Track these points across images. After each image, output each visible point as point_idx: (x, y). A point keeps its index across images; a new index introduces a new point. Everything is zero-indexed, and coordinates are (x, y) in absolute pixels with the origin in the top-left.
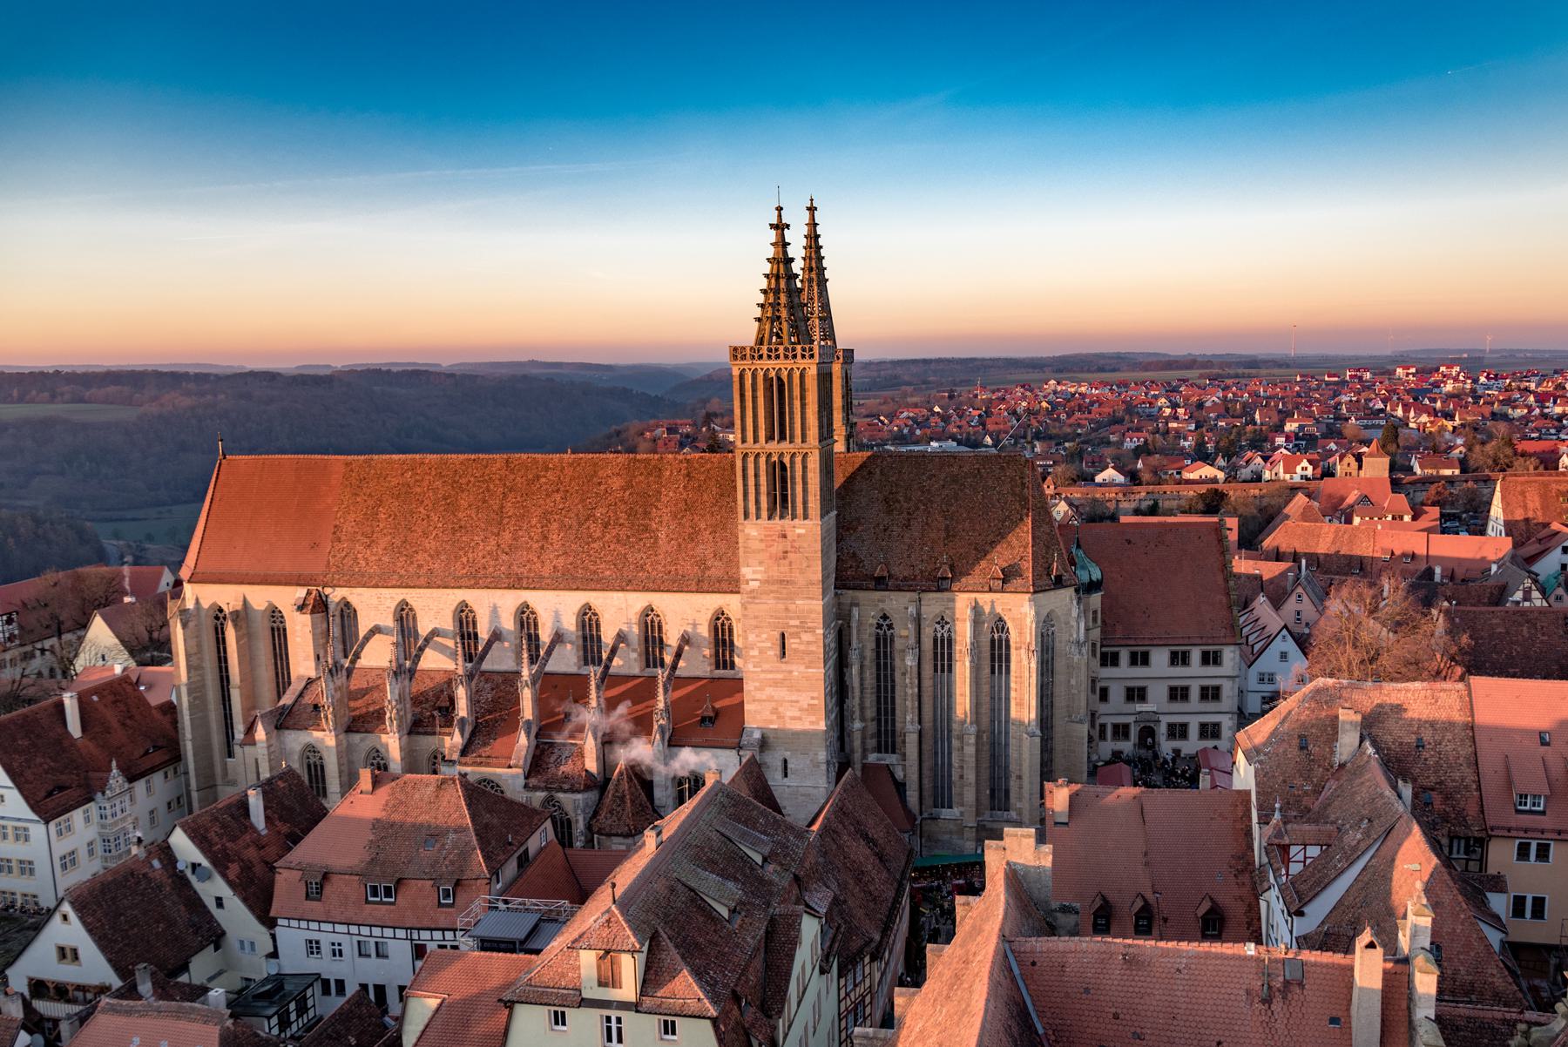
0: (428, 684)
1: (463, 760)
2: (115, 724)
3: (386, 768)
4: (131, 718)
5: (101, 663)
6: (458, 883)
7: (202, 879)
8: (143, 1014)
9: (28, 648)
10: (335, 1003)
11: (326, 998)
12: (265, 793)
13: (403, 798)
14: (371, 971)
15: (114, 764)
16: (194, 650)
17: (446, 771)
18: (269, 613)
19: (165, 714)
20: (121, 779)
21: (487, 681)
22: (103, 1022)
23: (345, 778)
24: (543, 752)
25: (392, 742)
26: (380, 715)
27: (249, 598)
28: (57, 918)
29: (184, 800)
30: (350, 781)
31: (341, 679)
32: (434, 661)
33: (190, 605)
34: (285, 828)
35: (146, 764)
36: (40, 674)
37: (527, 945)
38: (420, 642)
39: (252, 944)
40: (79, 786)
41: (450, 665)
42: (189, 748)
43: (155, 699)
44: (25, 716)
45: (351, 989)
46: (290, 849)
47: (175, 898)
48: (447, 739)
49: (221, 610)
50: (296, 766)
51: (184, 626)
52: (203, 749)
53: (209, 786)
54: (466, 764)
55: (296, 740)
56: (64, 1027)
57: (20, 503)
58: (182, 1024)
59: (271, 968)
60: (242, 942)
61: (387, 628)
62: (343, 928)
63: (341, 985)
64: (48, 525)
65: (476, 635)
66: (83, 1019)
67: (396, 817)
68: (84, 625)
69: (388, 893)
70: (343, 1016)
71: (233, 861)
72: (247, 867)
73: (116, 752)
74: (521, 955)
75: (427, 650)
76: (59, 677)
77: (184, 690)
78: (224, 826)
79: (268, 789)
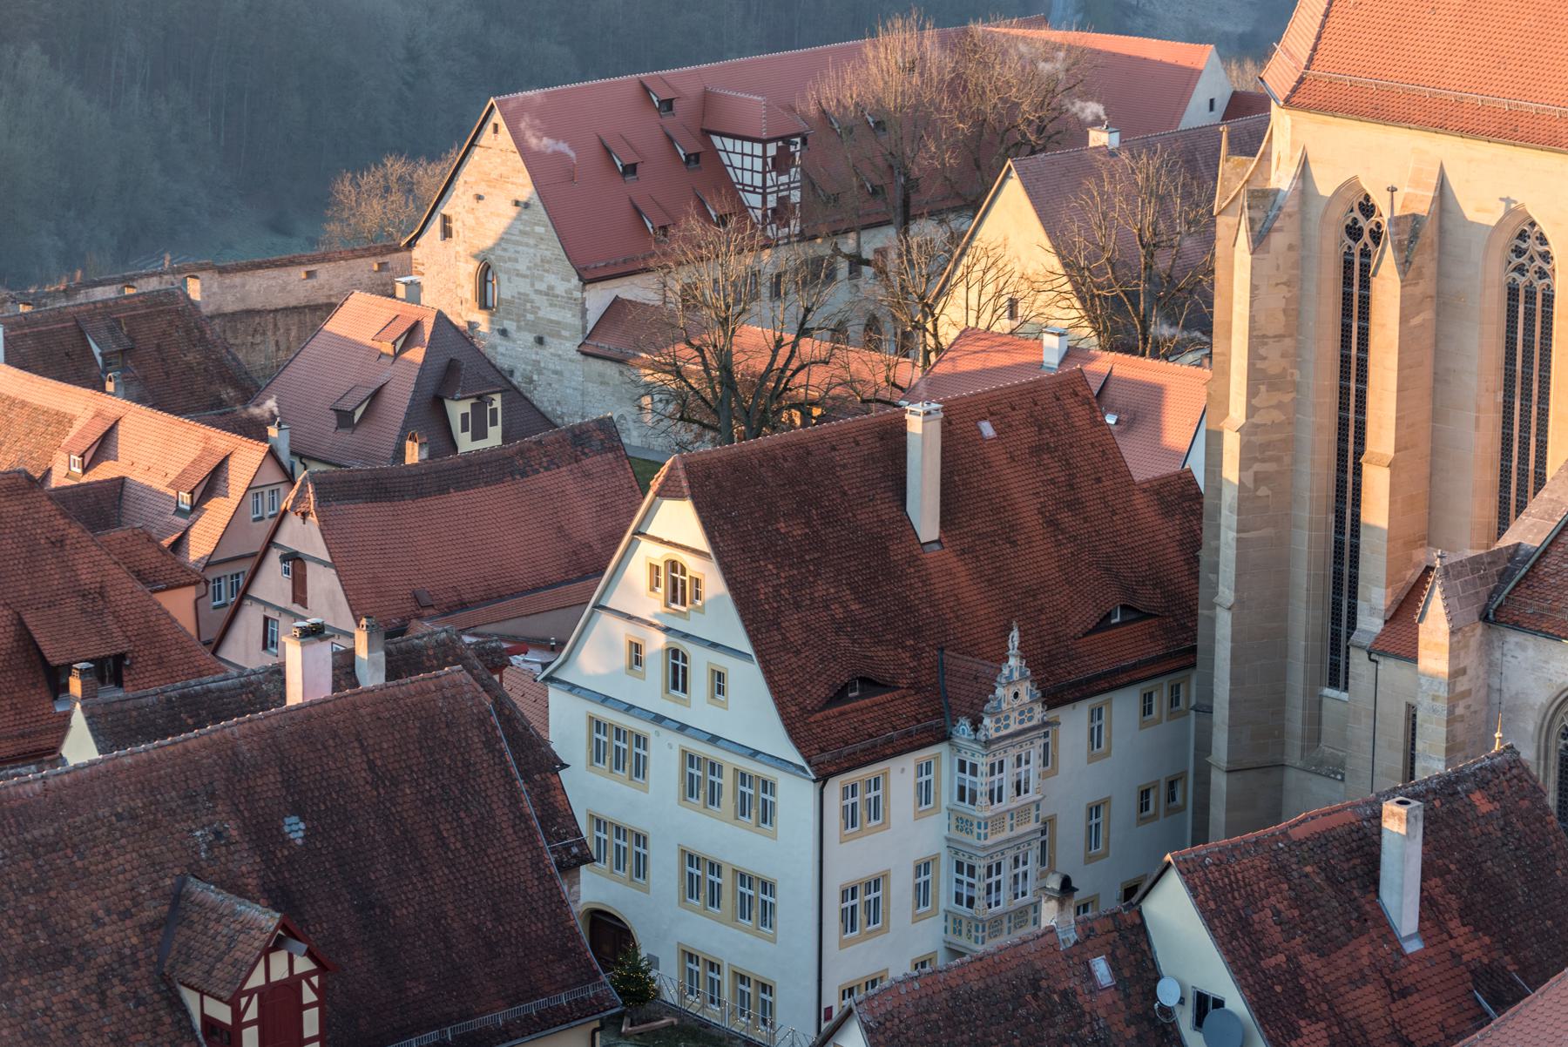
4: (1074, 505)
5: (1004, 325)
9: (821, 248)
15: (1015, 637)
16: (1277, 325)
18: (1506, 238)
19: (1167, 509)
20: (1025, 689)
33: (1282, 178)
34: (1474, 949)
40: (916, 687)
43: (1143, 466)
49: (1367, 209)
51: (1259, 240)
52: (1262, 649)
68: (970, 200)
71: (1314, 1017)
78: (1299, 900)
79: (1443, 808)
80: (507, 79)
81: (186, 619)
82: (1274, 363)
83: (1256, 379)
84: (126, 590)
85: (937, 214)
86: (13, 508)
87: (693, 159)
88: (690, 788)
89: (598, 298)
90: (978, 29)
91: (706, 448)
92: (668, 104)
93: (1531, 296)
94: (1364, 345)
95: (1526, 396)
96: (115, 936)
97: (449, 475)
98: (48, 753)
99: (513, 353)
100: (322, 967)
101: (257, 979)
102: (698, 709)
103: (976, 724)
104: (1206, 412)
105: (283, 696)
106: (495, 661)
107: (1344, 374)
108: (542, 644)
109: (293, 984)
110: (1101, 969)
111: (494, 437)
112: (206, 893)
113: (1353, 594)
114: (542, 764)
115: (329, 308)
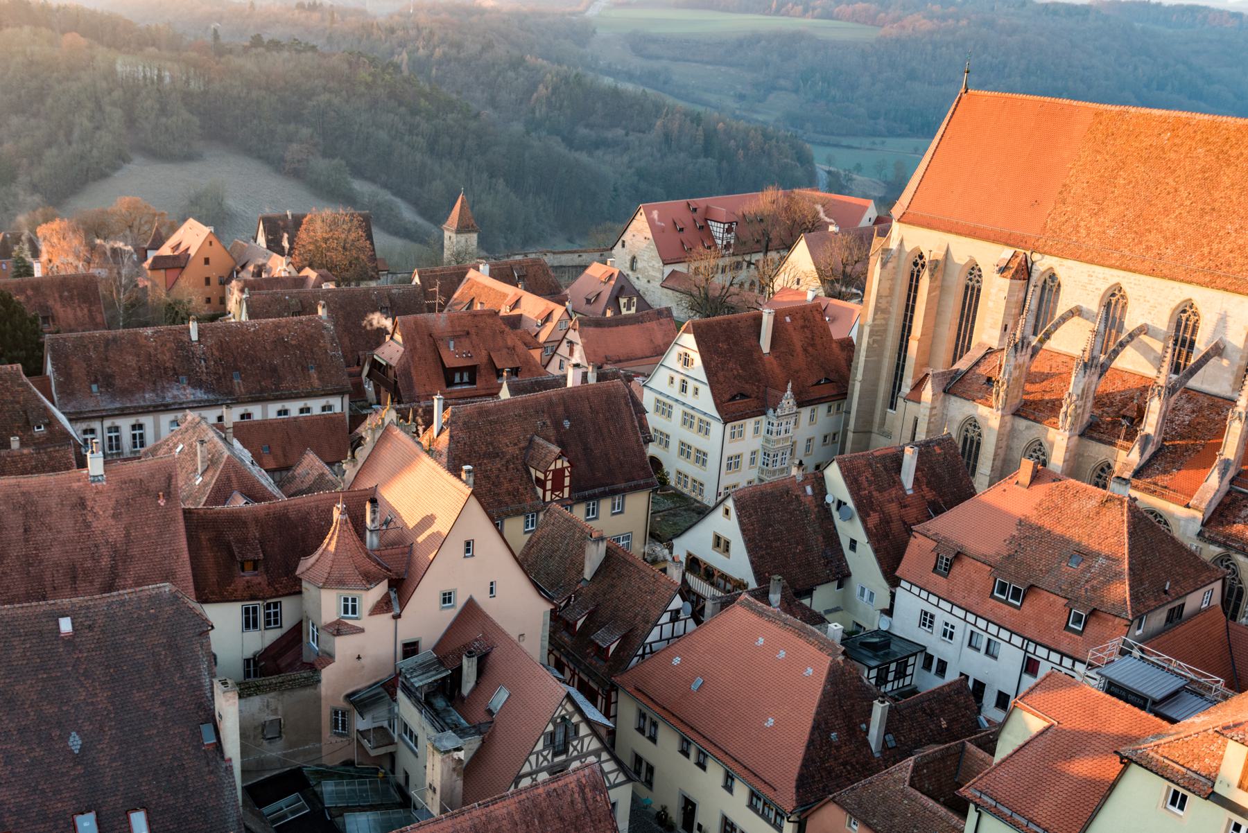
0: (1119, 386)
1: (1134, 482)
2: (799, 348)
3: (1044, 464)
4: (813, 345)
5: (795, 287)
6: (1093, 612)
7: (843, 518)
8: (772, 619)
9: (740, 259)
10: (930, 682)
11: (925, 672)
12: (920, 455)
13: (1060, 502)
14: (975, 665)
16: (885, 292)
17: (1115, 488)
18: (968, 269)
20: (792, 401)
21: (1189, 400)
22: (740, 615)
23: (999, 463)
24: (1234, 501)
25: (1059, 440)
26: (1053, 407)
27: (952, 249)
28: (721, 510)
29: (839, 438)
30: (1004, 470)
31: (1024, 357)
32: (1131, 362)
33: (894, 245)
34: (930, 495)
35: (816, 393)
36: (742, 285)
37: (1162, 708)
38: (1123, 337)
39: (872, 594)
40: (757, 398)
41: (1150, 372)
42: (856, 389)
43: (837, 333)
44: (729, 322)
45: (951, 676)
46: (929, 518)
47: (816, 526)
48: (1123, 453)
49: (921, 257)
50: (954, 436)
51: (884, 265)
53: (865, 431)
54: (1135, 488)
55: (960, 409)
56: (709, 605)
57: (755, 116)
58: (801, 642)
59: (883, 624)
60: (863, 589)
61: (1089, 311)
62: (961, 613)
63: (942, 667)
64: (774, 141)
65: (1192, 343)
66: (725, 604)
67: (1047, 523)
68: (789, 247)
69: (1016, 594)
70: (941, 696)
71: (875, 511)
72: (886, 521)
73: (792, 375)
74: (1151, 716)
75: (1128, 347)
76: (756, 291)
77: (867, 330)
79: (925, 450)
80: (645, 197)
81: (538, 358)
82: (883, 305)
83: (877, 309)
84: (521, 348)
85: (777, 250)
86: (490, 321)
87: (701, 228)
88: (684, 422)
89: (668, 270)
90: (797, 191)
91: (697, 318)
92: (695, 210)
93: (973, 288)
94: (914, 301)
95: (967, 321)
96: (512, 450)
97: (620, 321)
98: (495, 394)
99: (640, 284)
100: (572, 466)
101: (552, 467)
102: (689, 398)
103: (775, 411)
104: (858, 320)
105: (566, 384)
106: (629, 379)
107: (907, 310)
108: (643, 375)
109: (563, 470)
110: (809, 489)
111: (633, 310)
112: (538, 440)
113: (901, 380)
114: (641, 411)
115: (586, 267)
